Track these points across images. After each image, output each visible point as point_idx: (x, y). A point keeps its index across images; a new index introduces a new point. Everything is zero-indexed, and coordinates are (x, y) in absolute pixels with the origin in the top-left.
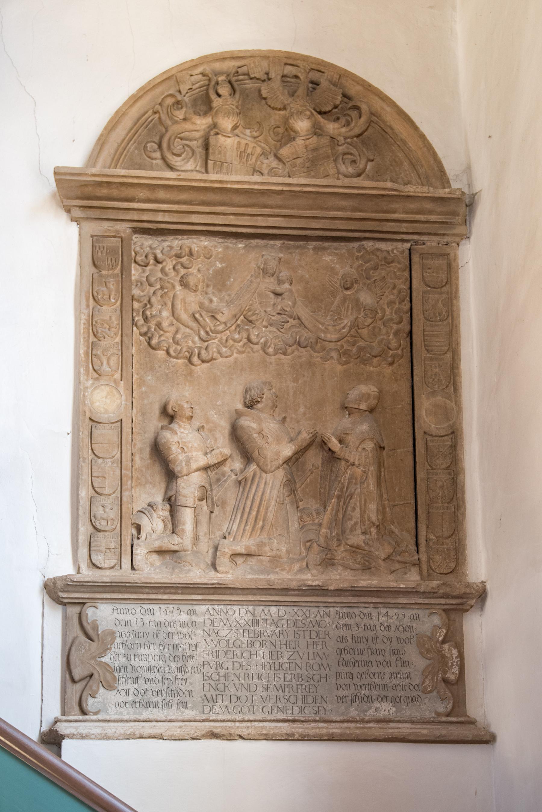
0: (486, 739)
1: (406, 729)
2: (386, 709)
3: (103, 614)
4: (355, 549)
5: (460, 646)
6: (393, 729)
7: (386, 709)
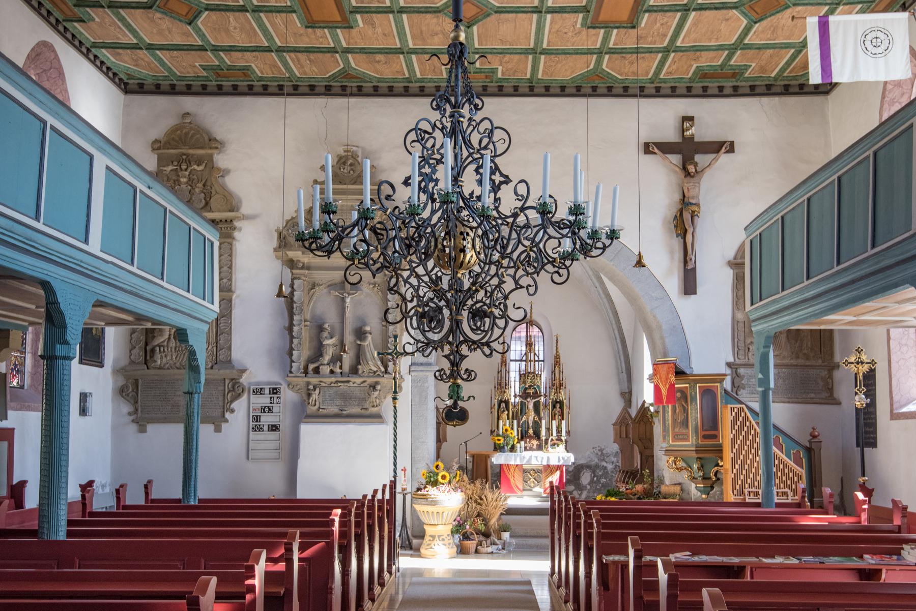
0: (839, 403)
1: (818, 400)
2: (813, 395)
3: (742, 371)
4: (805, 354)
5: (832, 379)
6: (815, 400)
7: (813, 395)
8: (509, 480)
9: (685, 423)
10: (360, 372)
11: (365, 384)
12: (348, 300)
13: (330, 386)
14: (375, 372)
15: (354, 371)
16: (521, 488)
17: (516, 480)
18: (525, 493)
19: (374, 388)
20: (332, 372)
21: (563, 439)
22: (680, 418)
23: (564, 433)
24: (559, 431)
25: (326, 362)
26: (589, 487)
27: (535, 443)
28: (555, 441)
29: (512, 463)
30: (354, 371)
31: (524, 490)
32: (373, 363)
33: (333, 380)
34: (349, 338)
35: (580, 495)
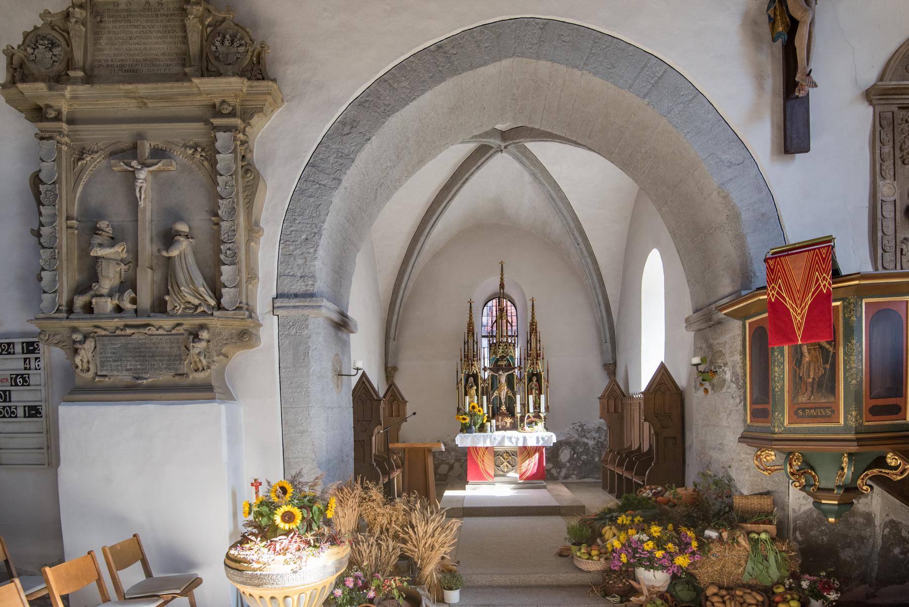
8: (477, 465)
9: (828, 384)
10: (169, 308)
11: (180, 330)
12: (143, 174)
13: (113, 335)
14: (196, 307)
15: (160, 307)
16: (492, 473)
17: (487, 465)
18: (496, 479)
19: (196, 337)
20: (119, 309)
21: (542, 415)
22: (812, 374)
23: (543, 409)
24: (537, 406)
25: (105, 291)
26: (568, 465)
27: (509, 421)
28: (532, 419)
29: (481, 445)
30: (160, 307)
31: (495, 476)
32: (192, 289)
33: (118, 322)
34: (148, 247)
35: (559, 473)
